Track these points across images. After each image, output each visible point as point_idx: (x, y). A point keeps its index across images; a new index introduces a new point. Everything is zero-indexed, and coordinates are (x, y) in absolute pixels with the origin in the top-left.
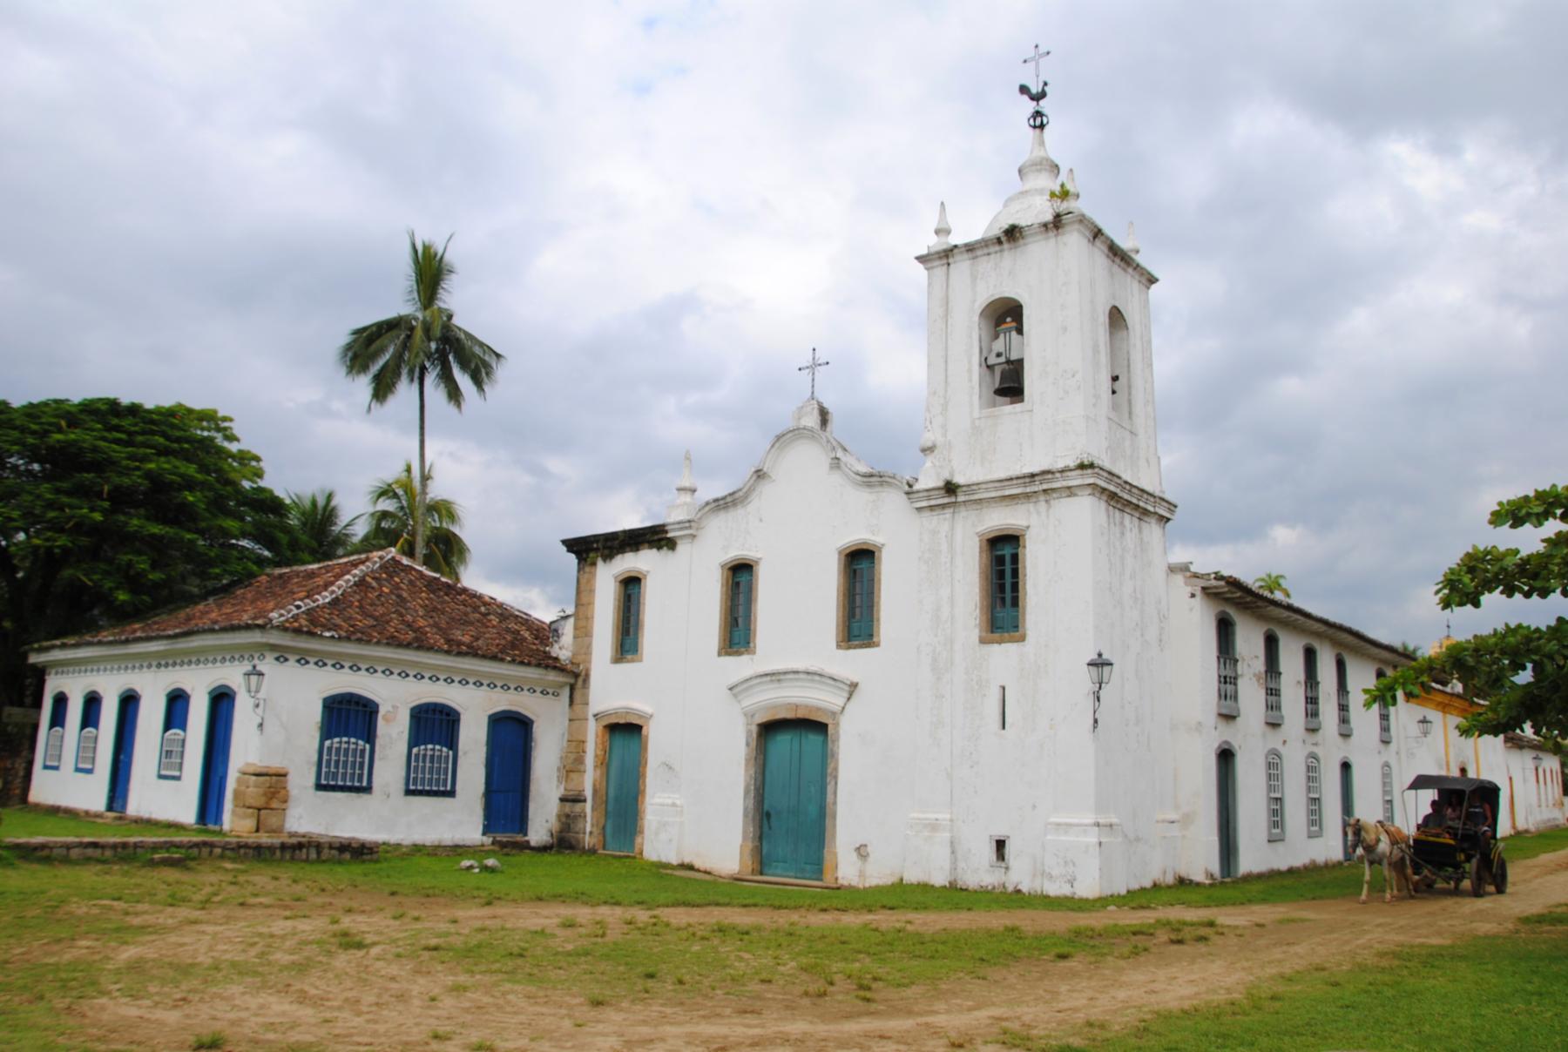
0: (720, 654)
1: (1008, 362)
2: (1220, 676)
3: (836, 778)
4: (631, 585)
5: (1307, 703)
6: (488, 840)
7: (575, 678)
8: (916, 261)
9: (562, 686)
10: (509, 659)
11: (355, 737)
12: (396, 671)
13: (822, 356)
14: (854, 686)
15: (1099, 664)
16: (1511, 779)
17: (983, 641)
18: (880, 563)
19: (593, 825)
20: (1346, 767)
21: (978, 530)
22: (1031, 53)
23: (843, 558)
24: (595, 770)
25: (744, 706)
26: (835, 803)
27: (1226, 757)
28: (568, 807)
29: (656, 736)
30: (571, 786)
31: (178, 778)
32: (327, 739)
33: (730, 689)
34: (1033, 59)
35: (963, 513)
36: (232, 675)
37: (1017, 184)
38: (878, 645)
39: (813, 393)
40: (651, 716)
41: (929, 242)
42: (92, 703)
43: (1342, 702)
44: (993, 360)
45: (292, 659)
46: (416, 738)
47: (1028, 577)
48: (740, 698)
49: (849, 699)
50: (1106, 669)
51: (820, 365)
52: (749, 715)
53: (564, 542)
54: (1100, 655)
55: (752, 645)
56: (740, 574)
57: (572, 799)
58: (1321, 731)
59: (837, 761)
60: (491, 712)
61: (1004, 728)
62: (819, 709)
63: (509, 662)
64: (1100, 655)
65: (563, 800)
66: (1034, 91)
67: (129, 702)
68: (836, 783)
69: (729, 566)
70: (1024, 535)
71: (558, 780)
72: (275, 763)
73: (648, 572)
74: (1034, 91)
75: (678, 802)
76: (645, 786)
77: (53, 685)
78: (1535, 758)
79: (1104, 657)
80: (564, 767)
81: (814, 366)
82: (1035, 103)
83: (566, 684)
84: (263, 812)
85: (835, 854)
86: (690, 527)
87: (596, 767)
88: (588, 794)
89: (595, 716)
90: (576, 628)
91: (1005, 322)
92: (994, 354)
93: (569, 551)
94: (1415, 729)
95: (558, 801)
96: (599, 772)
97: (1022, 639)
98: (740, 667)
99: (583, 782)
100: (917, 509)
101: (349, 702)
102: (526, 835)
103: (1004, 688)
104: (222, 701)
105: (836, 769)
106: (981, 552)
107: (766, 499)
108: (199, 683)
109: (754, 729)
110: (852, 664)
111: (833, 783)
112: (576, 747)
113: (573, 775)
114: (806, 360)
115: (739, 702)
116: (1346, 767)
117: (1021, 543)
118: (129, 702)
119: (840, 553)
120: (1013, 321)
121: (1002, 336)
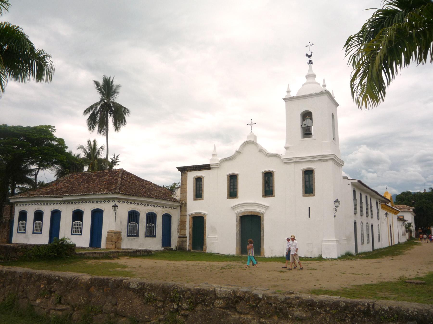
0: (227, 198)
1: (308, 127)
2: (354, 204)
3: (263, 230)
4: (199, 181)
5: (366, 210)
6: (163, 248)
7: (183, 205)
8: (283, 100)
9: (178, 206)
10: (169, 200)
11: (135, 222)
12: (99, 201)
13: (254, 122)
15: (337, 201)
16: (398, 228)
17: (303, 196)
18: (274, 176)
19: (189, 244)
20: (372, 226)
21: (301, 169)
22: (308, 44)
23: (263, 174)
24: (189, 229)
25: (235, 212)
26: (263, 236)
27: (355, 223)
28: (181, 239)
30: (181, 234)
31: (81, 235)
32: (129, 223)
33: (232, 207)
34: (308, 46)
37: (305, 80)
38: (274, 196)
39: (252, 131)
40: (207, 214)
41: (285, 95)
43: (367, 208)
44: (303, 126)
45: (121, 201)
46: (147, 222)
47: (315, 181)
48: (234, 210)
49: (266, 210)
50: (339, 203)
51: (253, 124)
53: (178, 168)
54: (337, 200)
55: (237, 196)
57: (182, 237)
58: (363, 216)
59: (264, 225)
60: (163, 214)
61: (310, 217)
62: (258, 213)
63: (169, 200)
64: (337, 200)
65: (179, 237)
66: (309, 55)
68: (263, 231)
69: (229, 175)
70: (314, 170)
71: (177, 232)
73: (204, 176)
74: (309, 55)
75: (216, 237)
76: (206, 233)
77: (18, 209)
78: (403, 223)
79: (338, 200)
80: (179, 228)
81: (252, 124)
82: (309, 58)
83: (180, 206)
84: (116, 243)
85: (264, 249)
86: (218, 165)
87: (190, 228)
88: (188, 235)
89: (189, 214)
90: (181, 191)
91: (306, 117)
92: (304, 124)
93: (179, 170)
94: (384, 216)
95: (178, 237)
96: (191, 229)
97: (314, 195)
98: (234, 202)
99: (186, 232)
100: (285, 163)
101: (134, 213)
102: (171, 247)
103: (309, 208)
105: (263, 227)
106: (302, 174)
107: (239, 158)
109: (239, 217)
110: (267, 201)
111: (263, 231)
112: (182, 224)
113: (182, 231)
114: (250, 122)
115: (234, 211)
116: (372, 226)
117: (313, 172)
119: (262, 173)
120: (309, 117)
121: (306, 120)
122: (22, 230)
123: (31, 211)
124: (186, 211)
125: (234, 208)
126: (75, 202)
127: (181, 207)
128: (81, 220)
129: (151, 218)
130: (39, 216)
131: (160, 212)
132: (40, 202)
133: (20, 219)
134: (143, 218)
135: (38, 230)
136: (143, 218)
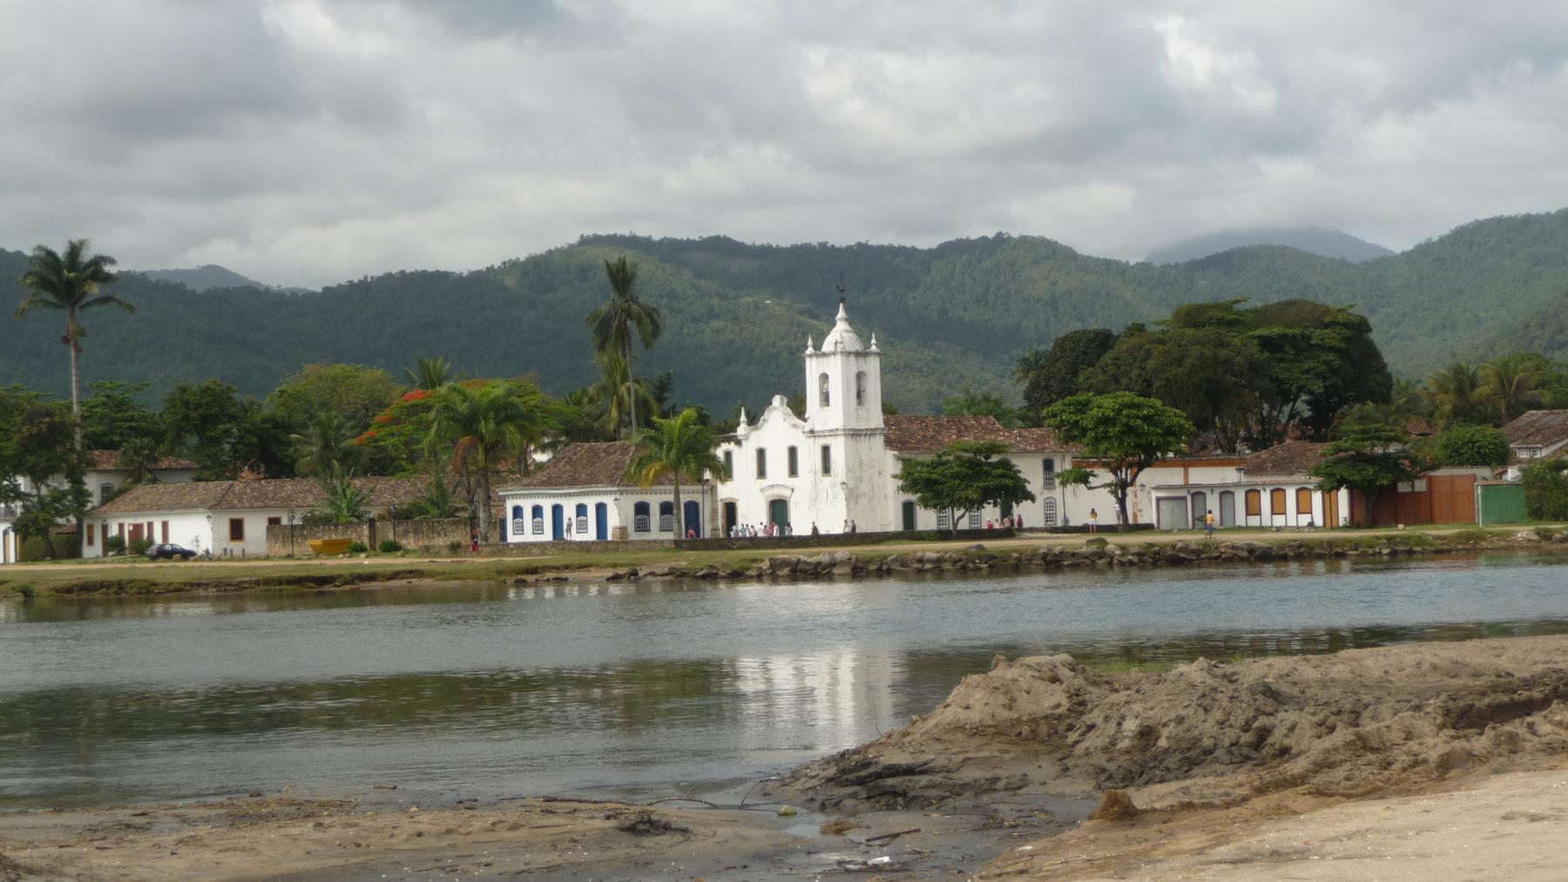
14: (793, 490)
36: (608, 500)
42: (537, 511)
52: (766, 498)
56: (761, 453)
65: (712, 530)
67: (557, 510)
72: (624, 525)
77: (510, 505)
98: (764, 483)
104: (601, 508)
108: (591, 503)
110: (792, 482)
112: (714, 511)
118: (557, 510)
122: (519, 529)
123: (527, 506)
125: (762, 490)
126: (577, 494)
128: (585, 515)
130: (537, 511)
132: (539, 496)
133: (515, 517)
135: (538, 529)
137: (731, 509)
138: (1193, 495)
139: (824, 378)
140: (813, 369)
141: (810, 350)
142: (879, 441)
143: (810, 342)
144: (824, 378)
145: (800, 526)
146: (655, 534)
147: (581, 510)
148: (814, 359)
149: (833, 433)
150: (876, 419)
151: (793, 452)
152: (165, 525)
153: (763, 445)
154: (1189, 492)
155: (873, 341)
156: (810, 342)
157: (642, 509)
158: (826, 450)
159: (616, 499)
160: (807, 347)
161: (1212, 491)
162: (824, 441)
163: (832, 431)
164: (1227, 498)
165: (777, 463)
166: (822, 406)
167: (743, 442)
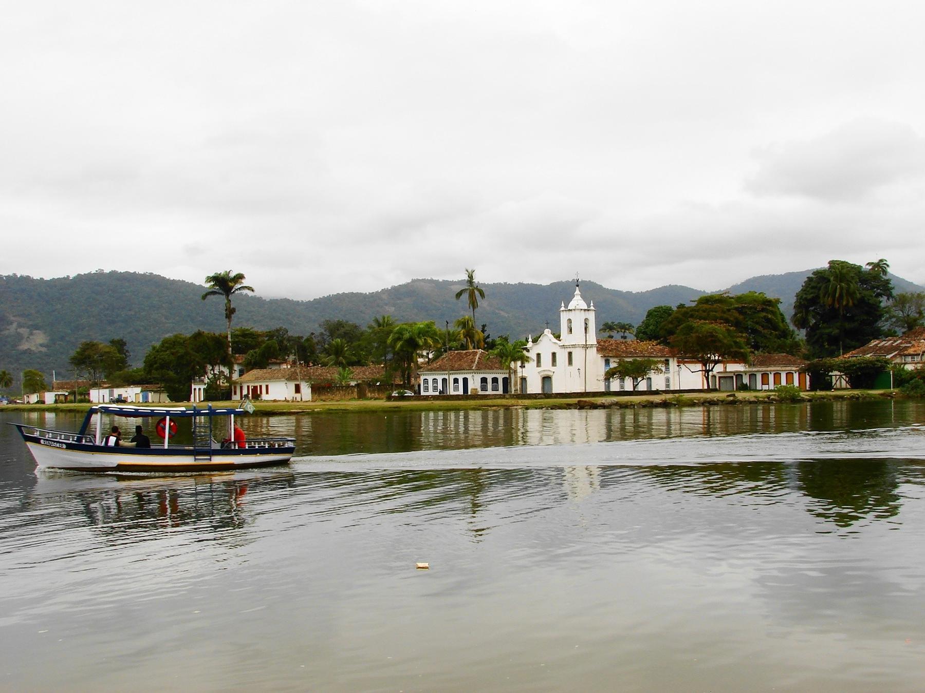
15: (579, 369)
29: (527, 379)
35: (566, 349)
77: (422, 378)
88: (519, 389)
98: (540, 369)
110: (553, 369)
122: (426, 389)
124: (517, 375)
127: (515, 372)
129: (495, 380)
131: (500, 377)
134: (490, 381)
136: (490, 381)
137: (524, 379)
138: (737, 376)
139: (570, 321)
140: (564, 317)
141: (563, 308)
142: (595, 349)
143: (563, 305)
144: (570, 321)
145: (557, 388)
146: (490, 392)
147: (456, 381)
148: (565, 312)
149: (574, 346)
150: (592, 339)
151: (554, 354)
152: (267, 386)
153: (540, 352)
154: (734, 374)
155: (592, 304)
156: (563, 305)
157: (484, 380)
158: (570, 354)
159: (473, 376)
160: (561, 307)
161: (746, 374)
162: (569, 350)
163: (574, 345)
164: (753, 377)
165: (546, 360)
166: (568, 334)
167: (530, 350)
